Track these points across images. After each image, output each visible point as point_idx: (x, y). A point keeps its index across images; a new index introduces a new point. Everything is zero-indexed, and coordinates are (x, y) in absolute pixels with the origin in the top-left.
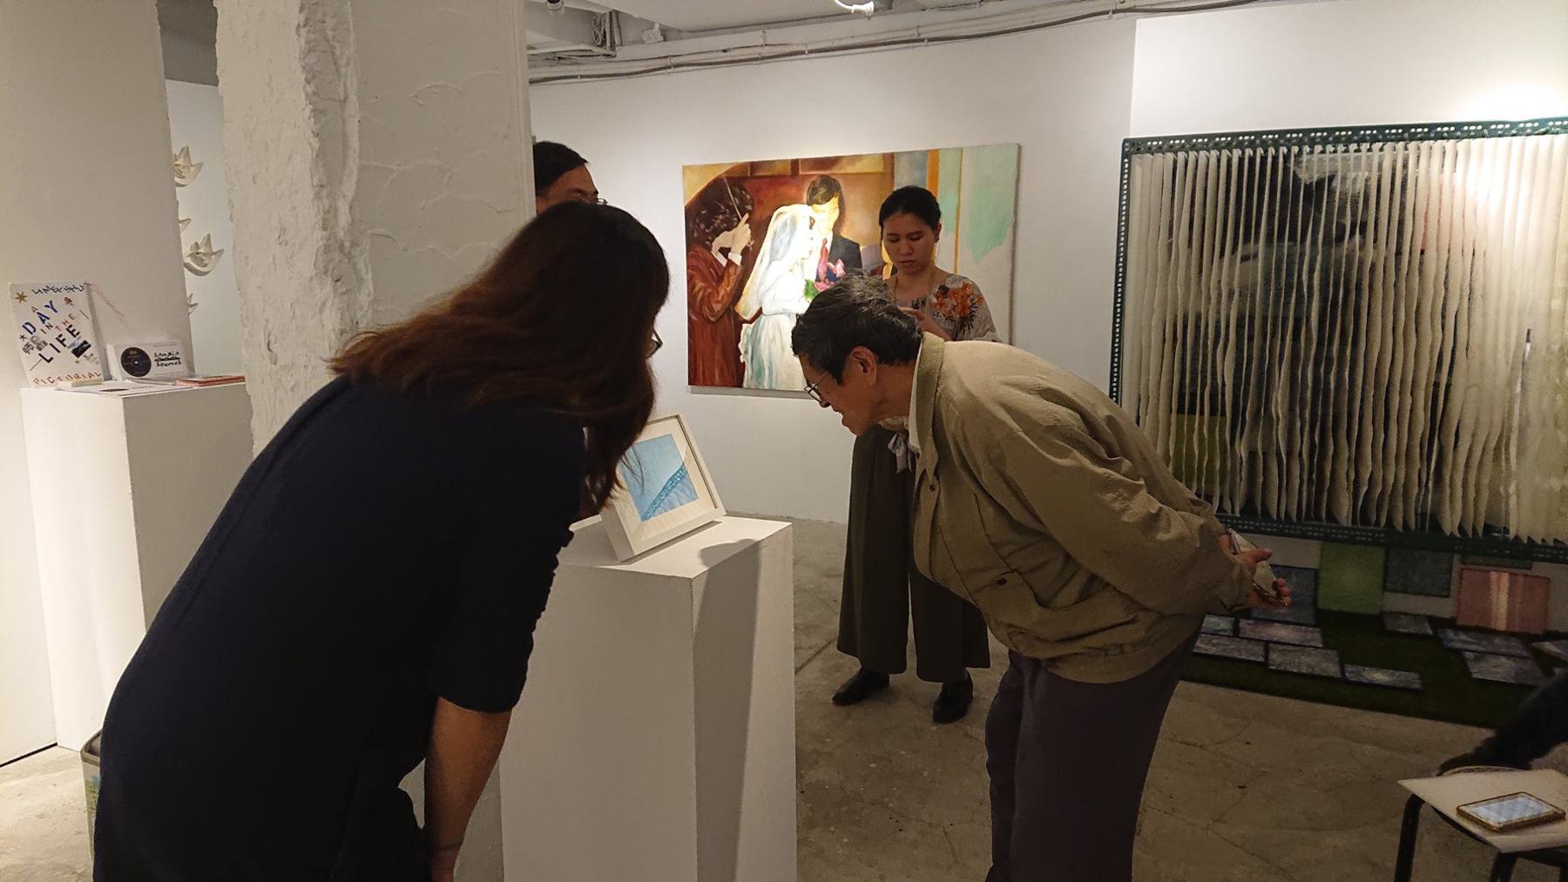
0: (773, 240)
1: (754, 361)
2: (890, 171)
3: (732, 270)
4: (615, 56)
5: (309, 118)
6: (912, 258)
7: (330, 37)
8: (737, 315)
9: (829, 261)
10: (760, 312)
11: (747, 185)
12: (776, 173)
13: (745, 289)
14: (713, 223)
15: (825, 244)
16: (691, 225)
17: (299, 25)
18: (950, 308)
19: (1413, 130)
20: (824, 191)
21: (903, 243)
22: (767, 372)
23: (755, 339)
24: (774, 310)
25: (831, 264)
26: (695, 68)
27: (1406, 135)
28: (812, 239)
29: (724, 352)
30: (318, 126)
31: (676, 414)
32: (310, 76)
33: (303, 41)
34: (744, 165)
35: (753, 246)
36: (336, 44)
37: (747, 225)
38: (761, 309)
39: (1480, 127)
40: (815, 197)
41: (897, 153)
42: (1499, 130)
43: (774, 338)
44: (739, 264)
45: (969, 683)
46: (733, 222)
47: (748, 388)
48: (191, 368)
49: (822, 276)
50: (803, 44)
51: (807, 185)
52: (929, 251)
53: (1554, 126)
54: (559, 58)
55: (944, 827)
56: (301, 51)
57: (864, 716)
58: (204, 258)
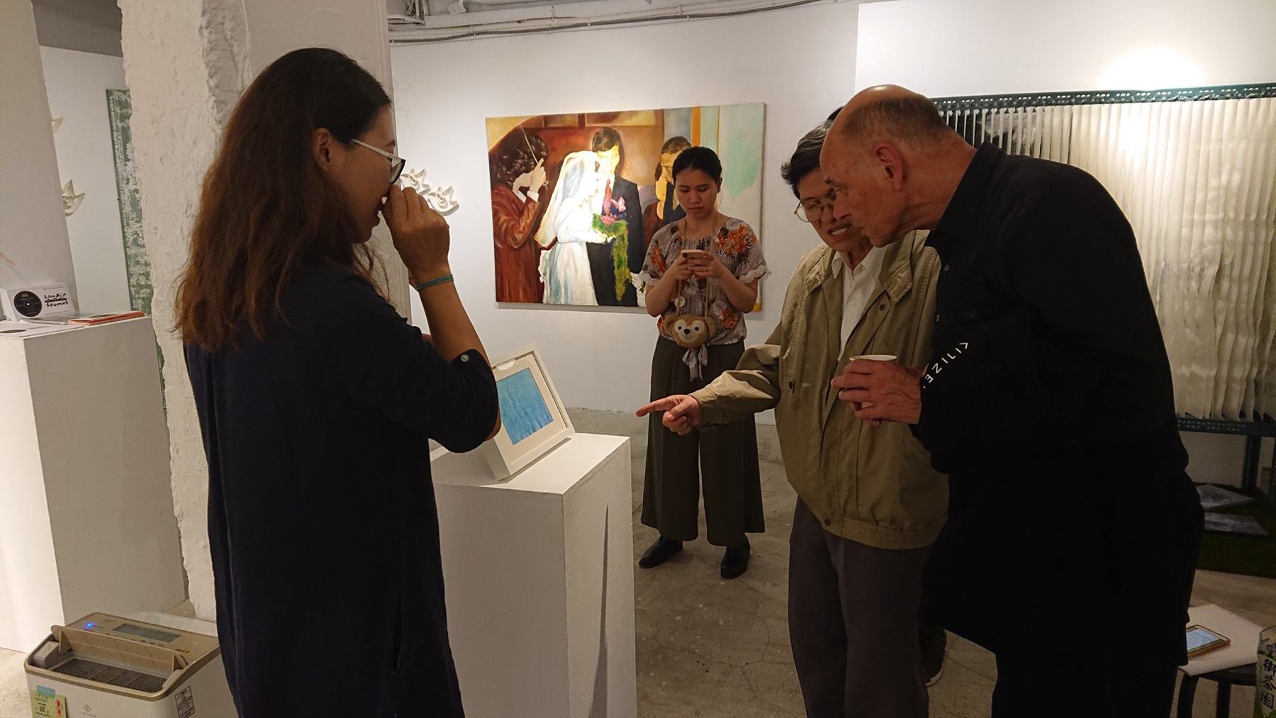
1: (552, 280)
2: (660, 124)
3: (530, 206)
5: (213, 108)
6: (701, 205)
7: (229, 37)
8: (536, 243)
9: (613, 198)
10: (556, 240)
11: (541, 135)
12: (566, 125)
14: (513, 167)
15: (608, 184)
16: (495, 168)
17: (201, 27)
18: (729, 246)
19: (1078, 96)
21: (693, 194)
22: (563, 291)
23: (552, 263)
25: (614, 201)
26: (494, 35)
27: (1073, 100)
28: (597, 180)
29: (527, 278)
30: (221, 115)
31: (530, 351)
32: (213, 70)
33: (206, 40)
34: (538, 118)
35: (548, 186)
36: (235, 44)
37: (543, 168)
38: (556, 238)
39: (1128, 95)
40: (600, 145)
42: (1142, 97)
43: (569, 262)
45: (747, 546)
46: (532, 165)
47: (548, 304)
48: (77, 307)
49: (607, 211)
50: (585, 18)
51: (592, 135)
52: (713, 199)
53: (1181, 95)
55: (741, 667)
56: (204, 49)
57: (667, 576)
58: (67, 201)
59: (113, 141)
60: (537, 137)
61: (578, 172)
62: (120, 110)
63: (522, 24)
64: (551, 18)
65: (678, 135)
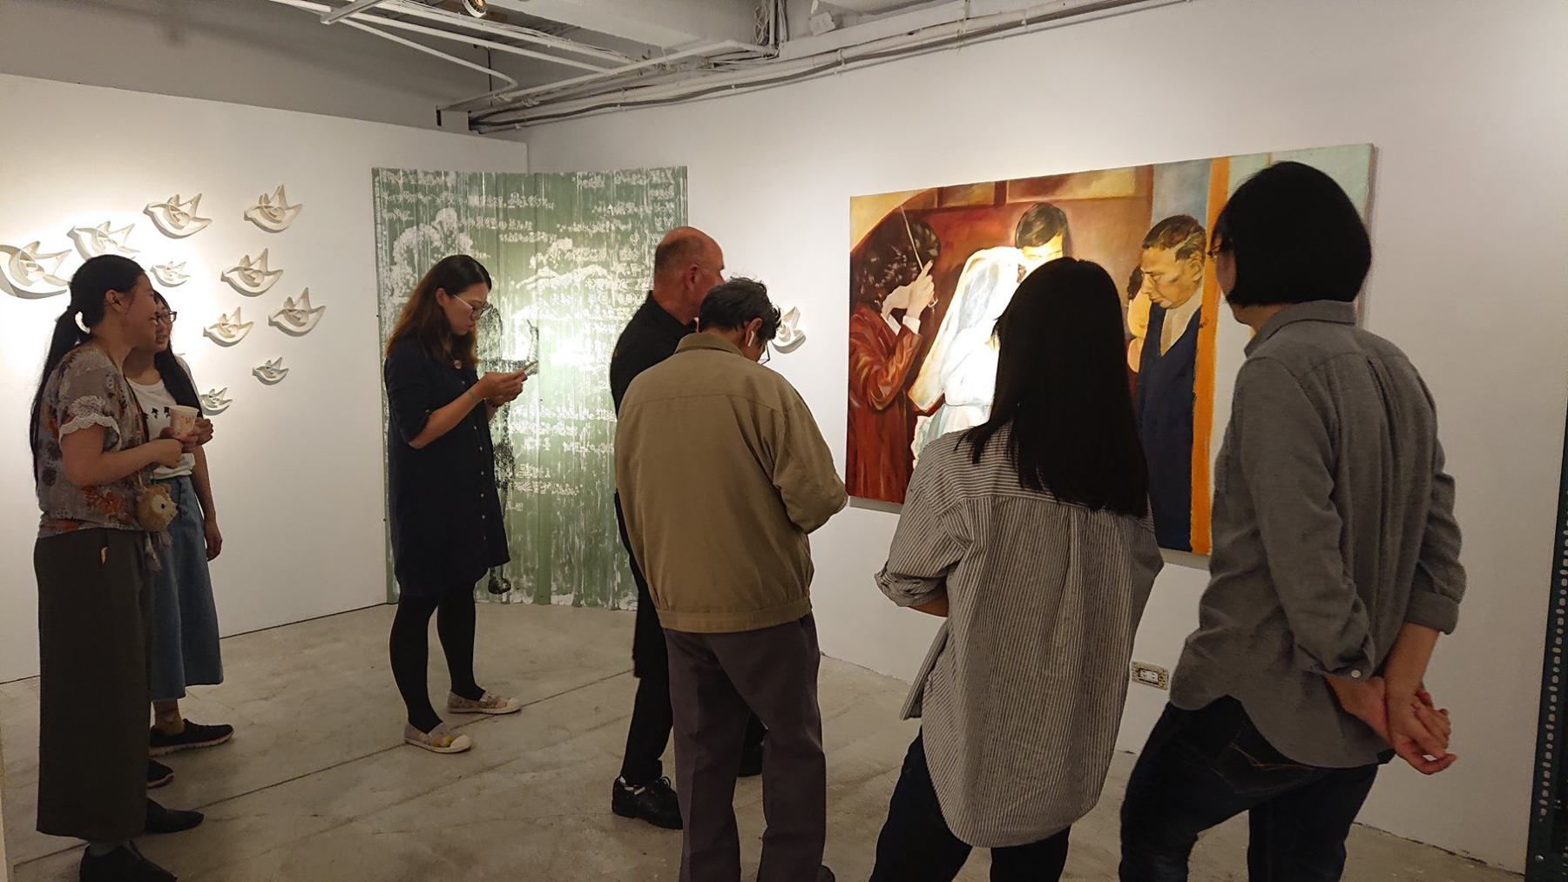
0: (964, 298)
2: (1144, 193)
3: (906, 340)
4: (778, 56)
8: (910, 404)
10: (941, 401)
13: (923, 367)
16: (857, 278)
20: (1041, 227)
24: (960, 400)
34: (930, 192)
35: (935, 307)
37: (930, 277)
38: (943, 396)
40: (1028, 236)
41: (1158, 165)
44: (916, 331)
46: (912, 272)
51: (1016, 219)
54: (716, 65)
59: (376, 238)
60: (925, 226)
61: (987, 281)
62: (389, 195)
63: (915, 35)
64: (962, 20)
65: (1179, 213)
